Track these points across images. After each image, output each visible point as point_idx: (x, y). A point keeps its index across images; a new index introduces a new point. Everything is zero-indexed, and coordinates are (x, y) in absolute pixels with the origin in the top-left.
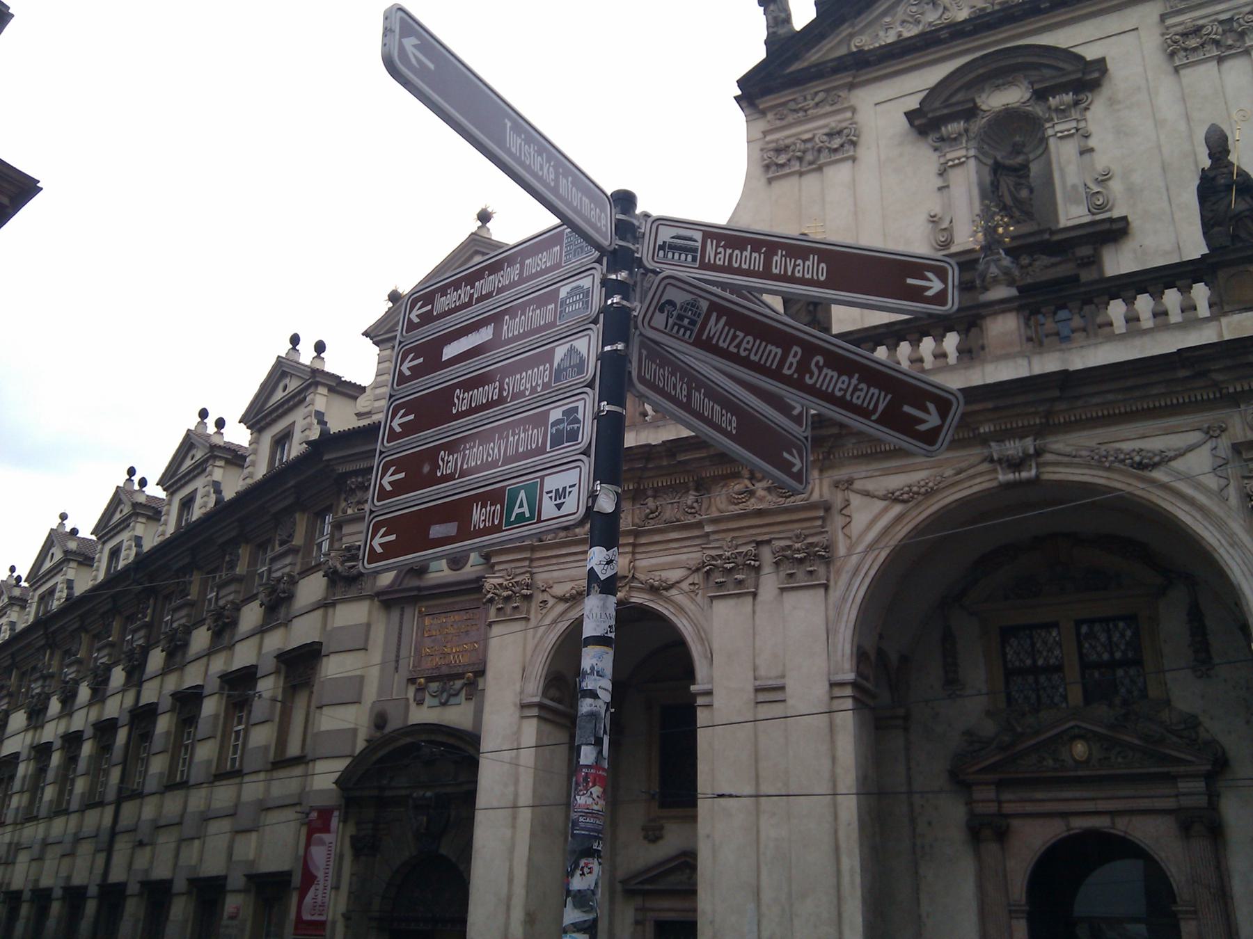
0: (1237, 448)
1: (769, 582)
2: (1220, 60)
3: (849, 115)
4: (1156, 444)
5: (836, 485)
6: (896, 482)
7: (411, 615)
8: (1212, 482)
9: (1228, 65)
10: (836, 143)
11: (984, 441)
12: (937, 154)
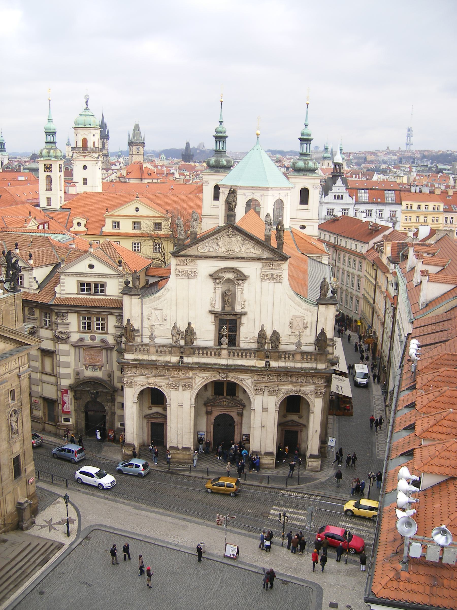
0: (255, 380)
1: (181, 388)
3: (196, 267)
5: (194, 374)
7: (82, 351)
8: (250, 385)
9: (270, 283)
10: (193, 274)
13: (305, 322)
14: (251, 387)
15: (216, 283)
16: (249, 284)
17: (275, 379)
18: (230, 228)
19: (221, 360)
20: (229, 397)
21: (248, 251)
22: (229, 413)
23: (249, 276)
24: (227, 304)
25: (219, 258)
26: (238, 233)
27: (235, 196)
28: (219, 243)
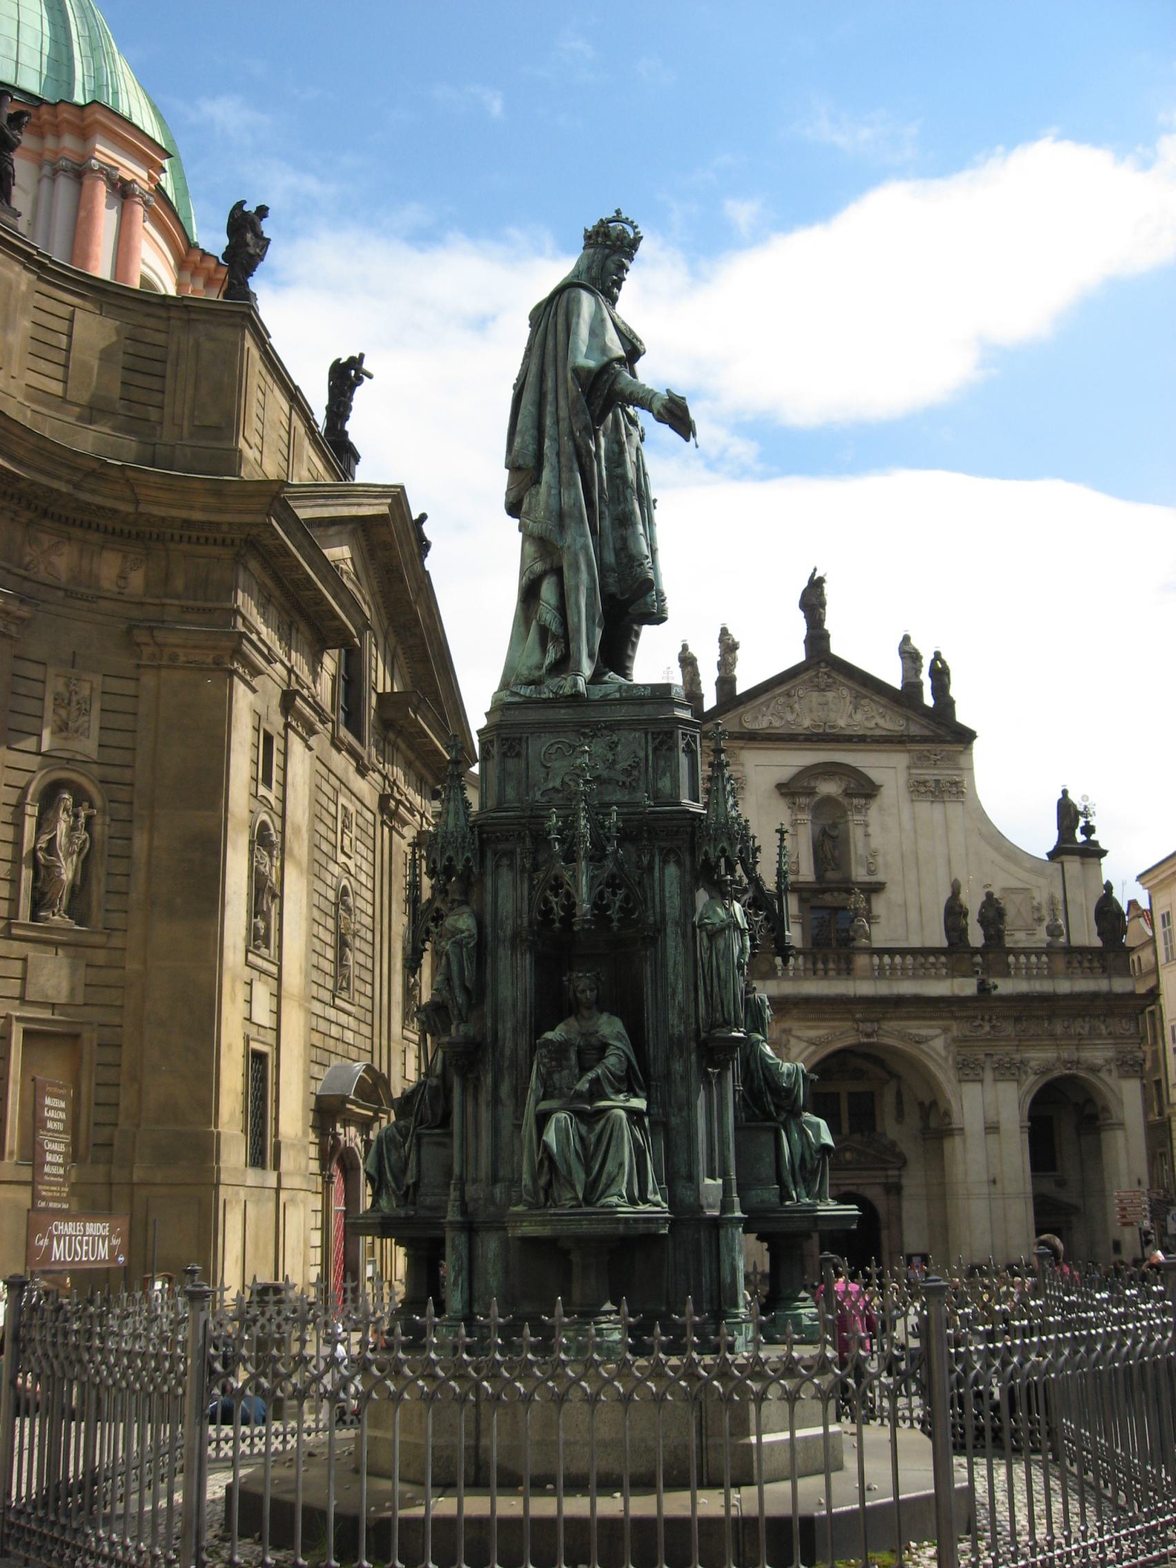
0: (954, 1040)
2: (932, 802)
3: (741, 769)
4: (924, 1032)
6: (812, 1033)
8: (943, 1053)
11: (856, 1021)
12: (789, 811)
13: (1035, 903)
14: (946, 1059)
15: (793, 806)
16: (881, 809)
17: (1009, 1029)
18: (823, 664)
19: (858, 983)
20: (857, 1137)
21: (872, 725)
22: (861, 1191)
23: (881, 786)
24: (829, 865)
25: (802, 738)
26: (841, 678)
27: (822, 594)
28: (797, 706)
